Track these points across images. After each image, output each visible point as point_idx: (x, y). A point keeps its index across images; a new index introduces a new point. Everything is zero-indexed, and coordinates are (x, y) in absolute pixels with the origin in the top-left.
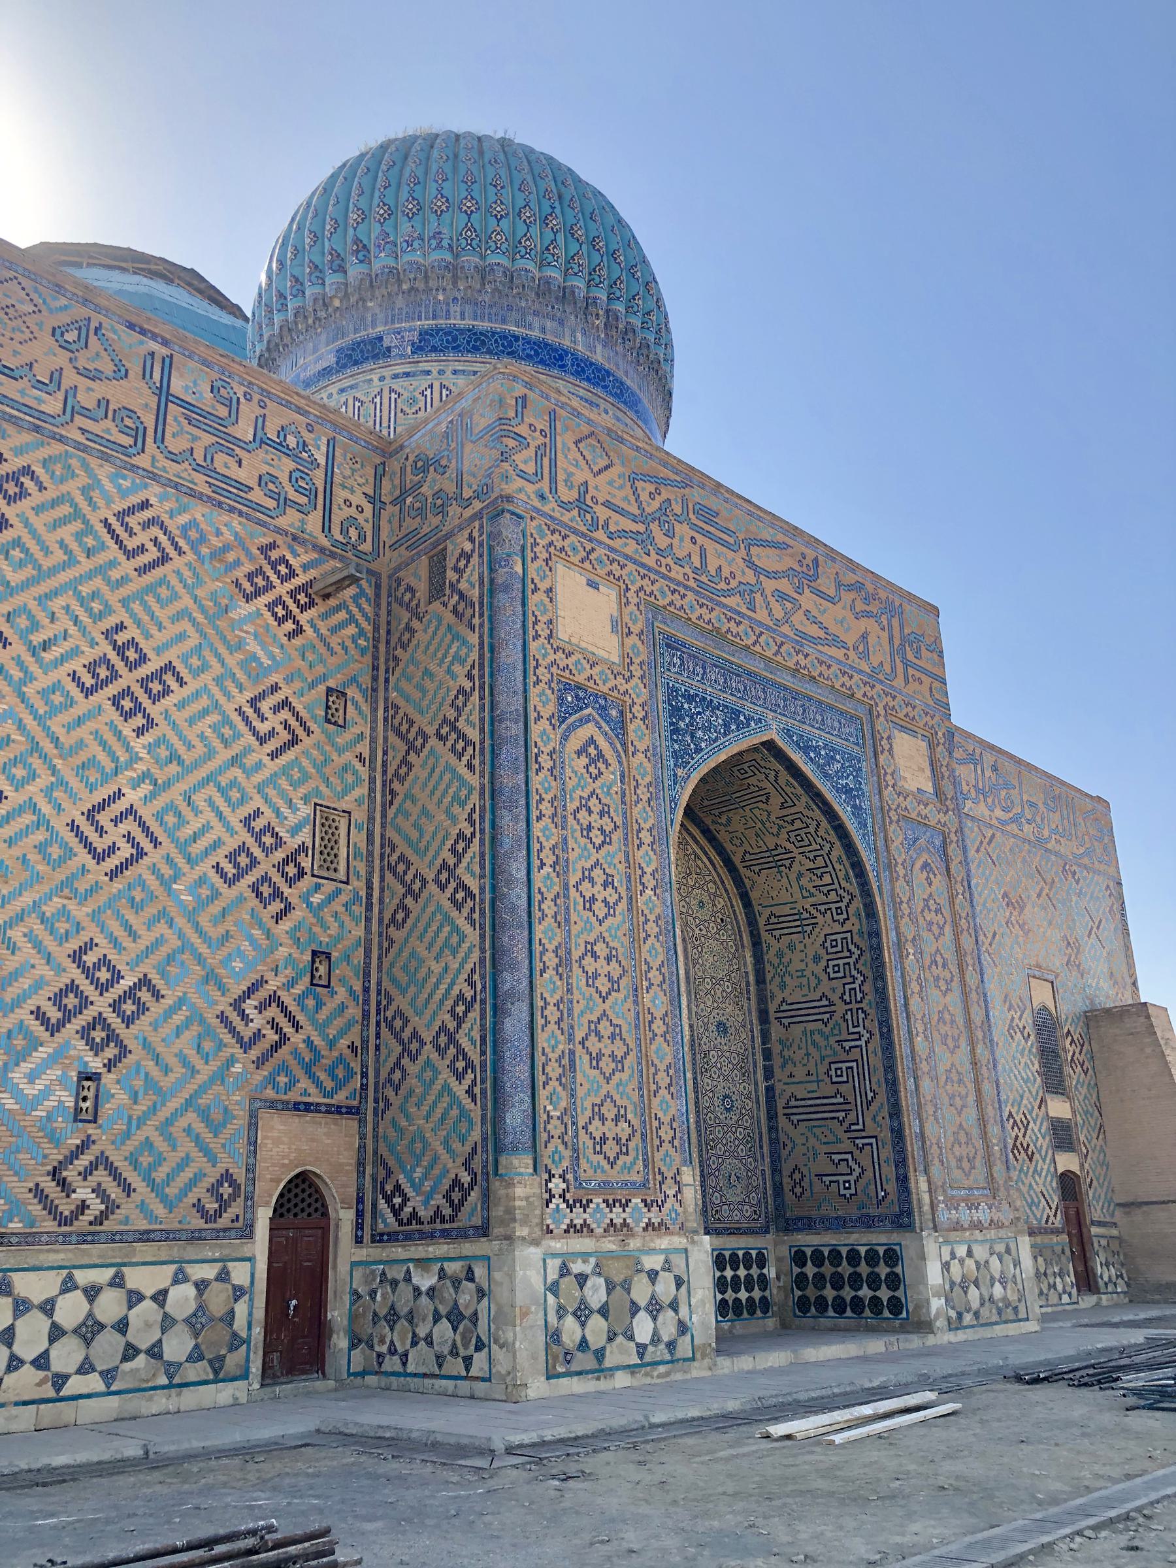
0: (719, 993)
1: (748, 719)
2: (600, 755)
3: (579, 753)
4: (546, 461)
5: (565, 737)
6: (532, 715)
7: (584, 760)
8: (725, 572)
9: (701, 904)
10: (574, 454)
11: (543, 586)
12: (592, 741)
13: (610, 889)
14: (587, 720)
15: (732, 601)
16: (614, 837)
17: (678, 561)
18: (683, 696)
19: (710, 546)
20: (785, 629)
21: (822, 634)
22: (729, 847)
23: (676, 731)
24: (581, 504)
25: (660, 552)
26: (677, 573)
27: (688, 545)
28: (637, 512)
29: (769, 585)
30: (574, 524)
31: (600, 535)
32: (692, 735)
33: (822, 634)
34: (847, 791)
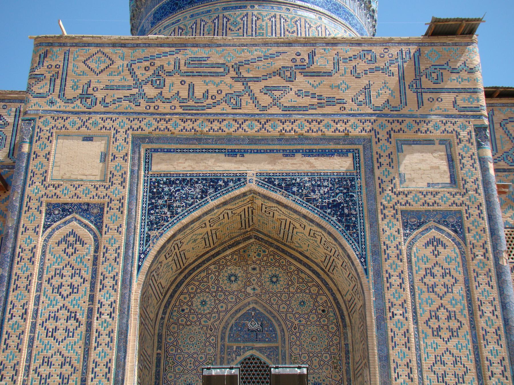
0: (316, 363)
1: (226, 184)
2: (79, 239)
3: (58, 244)
4: (58, 81)
5: (50, 236)
6: (21, 229)
7: (63, 246)
8: (213, 91)
9: (302, 303)
10: (83, 67)
11: (42, 154)
12: (72, 233)
13: (72, 321)
14: (70, 221)
15: (217, 110)
16: (82, 289)
17: (168, 100)
18: (165, 183)
19: (197, 82)
20: (274, 110)
21: (315, 101)
22: (315, 260)
23: (154, 206)
24: (84, 96)
25: (151, 100)
26: (164, 108)
27: (177, 87)
28: (131, 82)
29: (256, 88)
30: (77, 109)
31: (99, 107)
32: (170, 207)
33: (315, 101)
34: (335, 206)
